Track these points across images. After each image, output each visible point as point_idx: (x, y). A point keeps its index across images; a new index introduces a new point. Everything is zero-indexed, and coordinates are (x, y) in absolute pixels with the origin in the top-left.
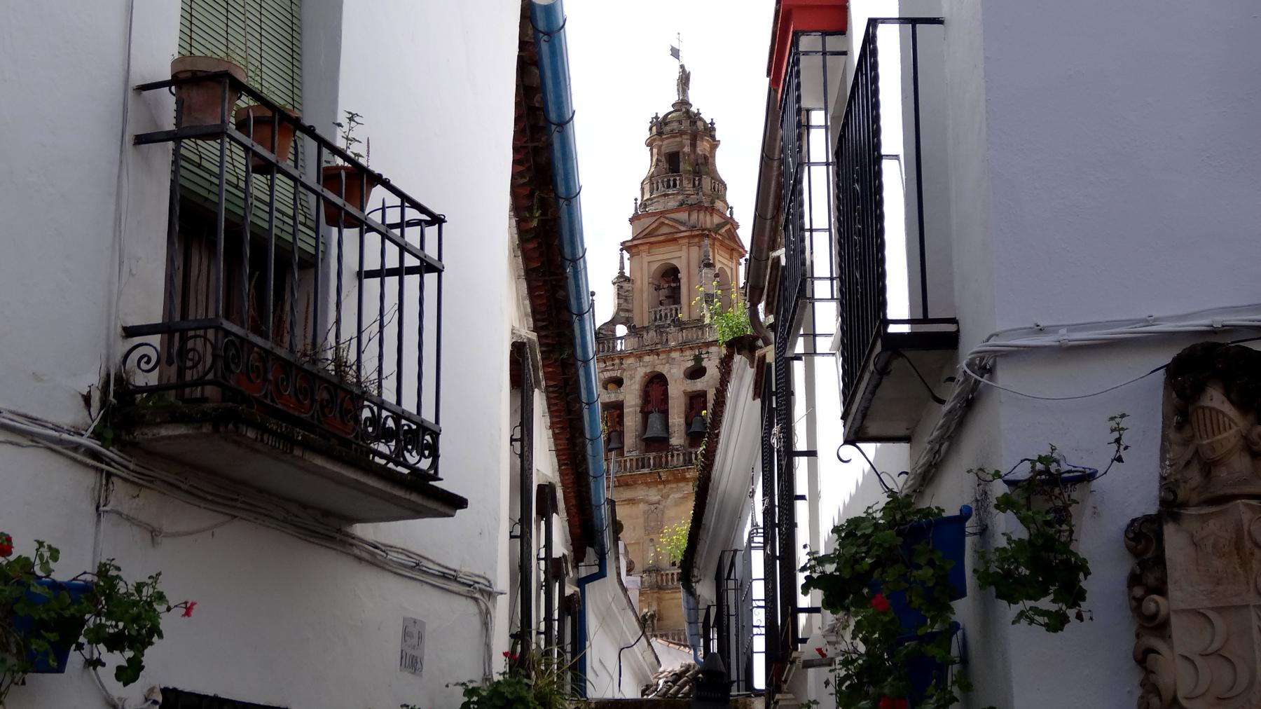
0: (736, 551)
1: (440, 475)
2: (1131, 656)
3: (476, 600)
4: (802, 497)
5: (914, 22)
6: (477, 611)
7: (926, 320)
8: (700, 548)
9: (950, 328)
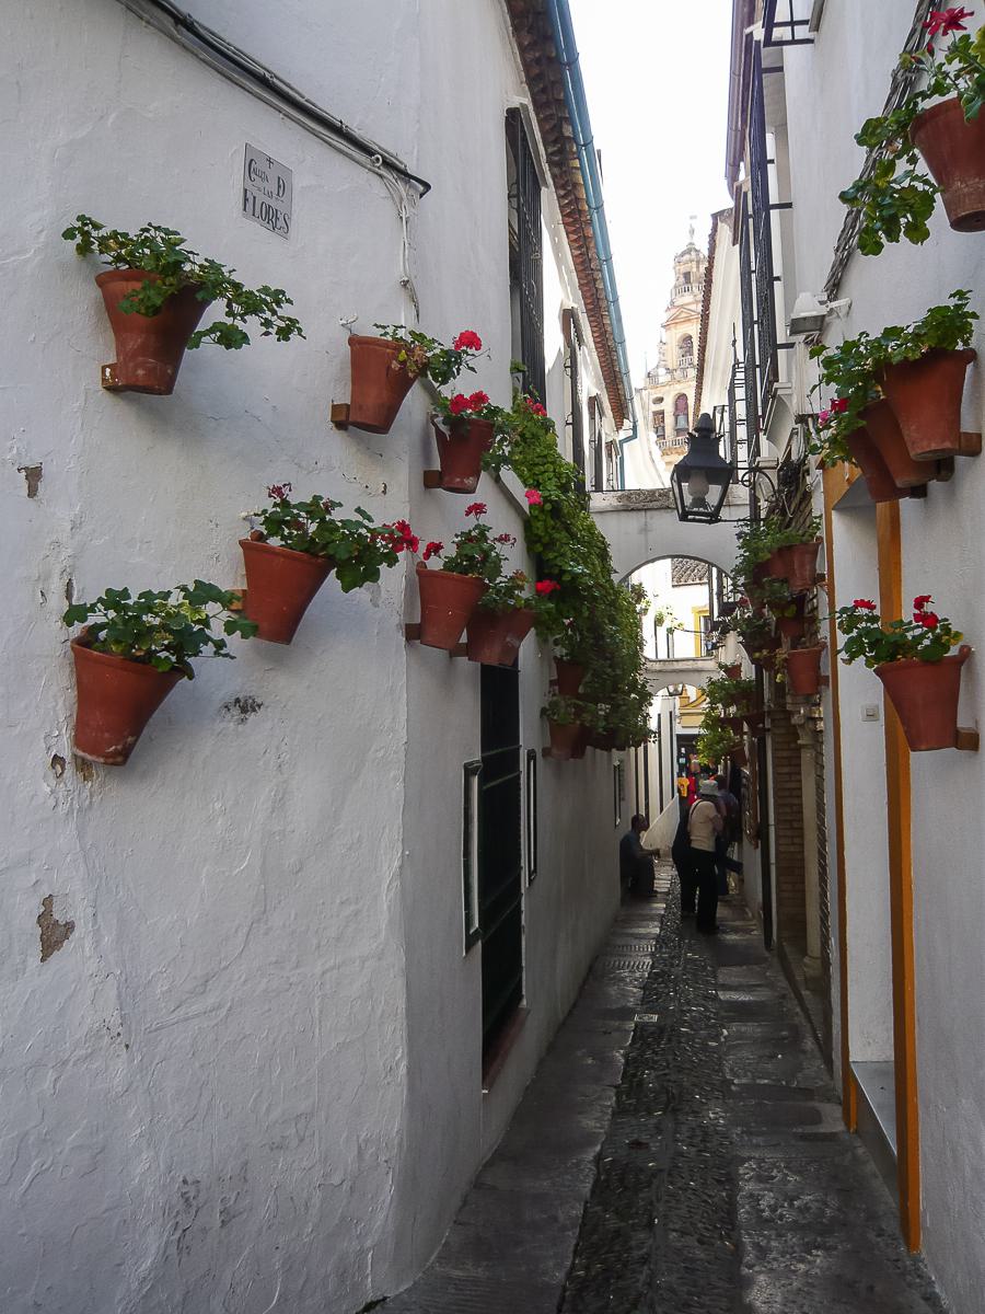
3: (381, 176)
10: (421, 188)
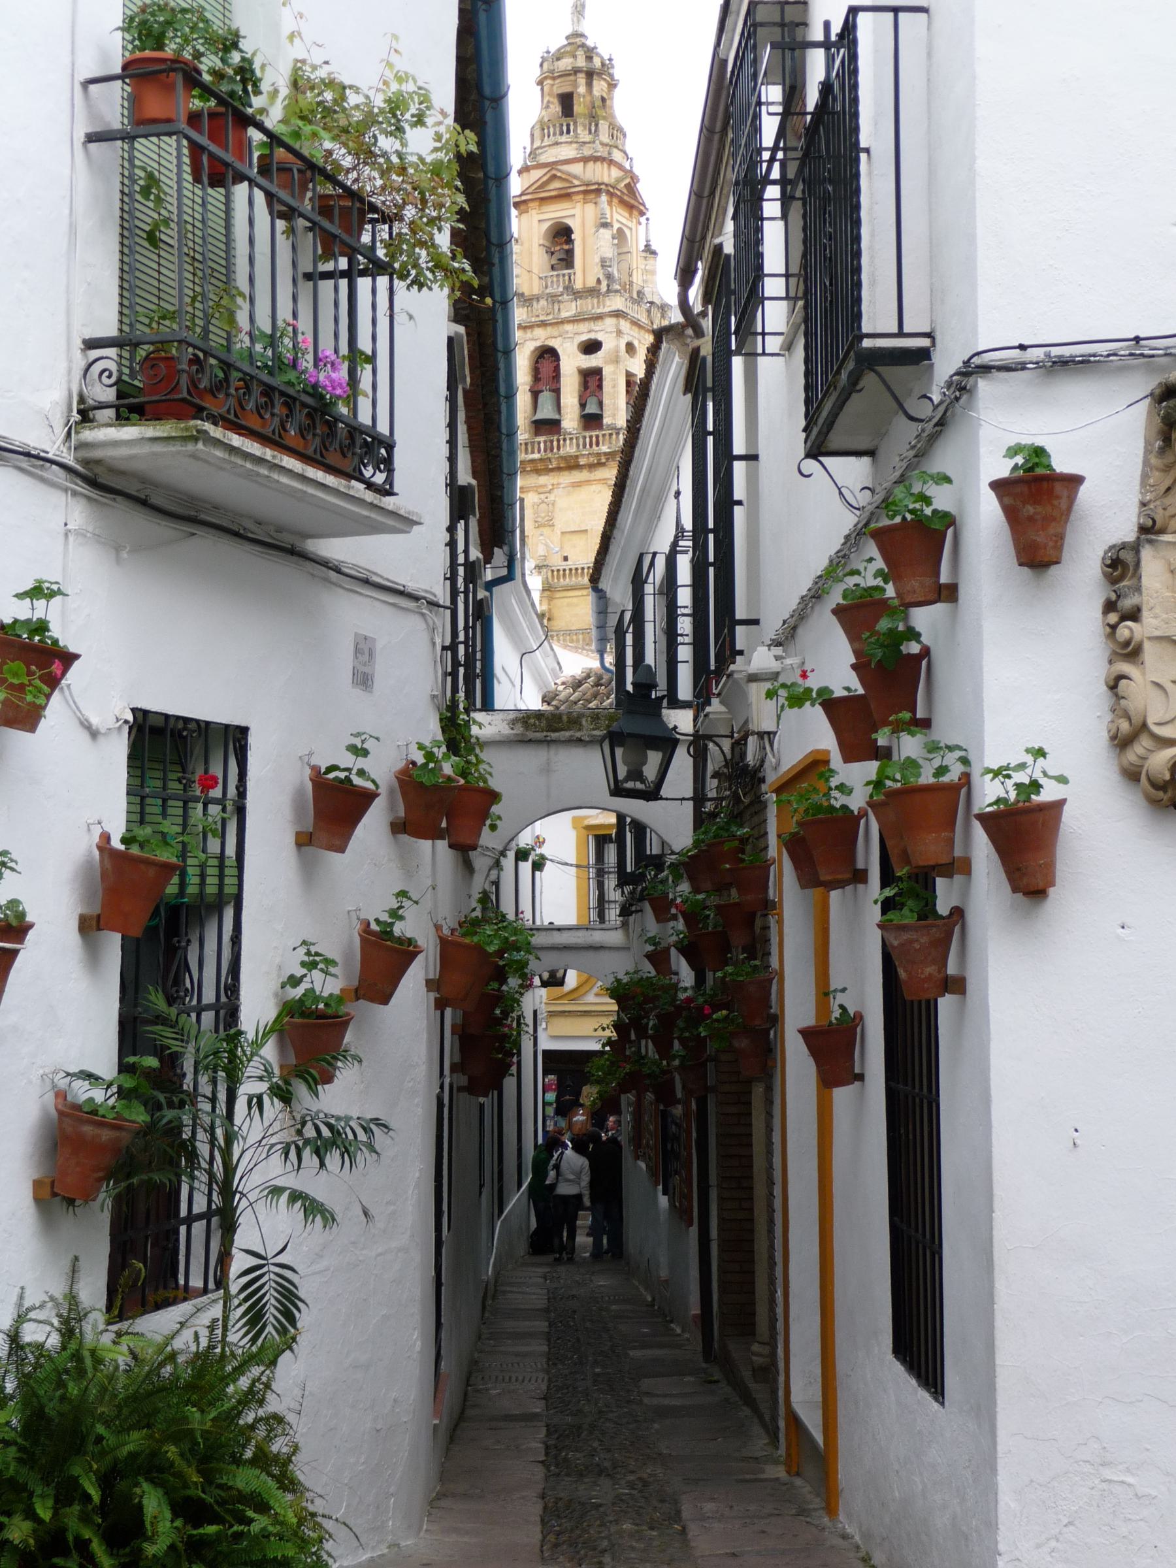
0: (654, 554)
1: (396, 490)
2: (1103, 682)
3: (423, 615)
4: (740, 503)
5: (896, 10)
6: (424, 626)
7: (901, 334)
8: (612, 548)
9: (924, 342)
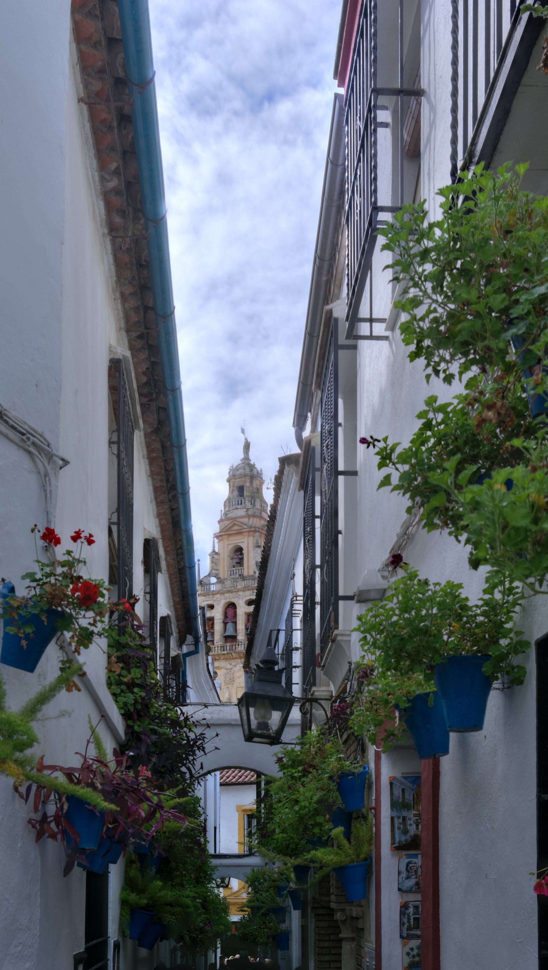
0: (279, 631)
3: (30, 453)
10: (61, 462)
